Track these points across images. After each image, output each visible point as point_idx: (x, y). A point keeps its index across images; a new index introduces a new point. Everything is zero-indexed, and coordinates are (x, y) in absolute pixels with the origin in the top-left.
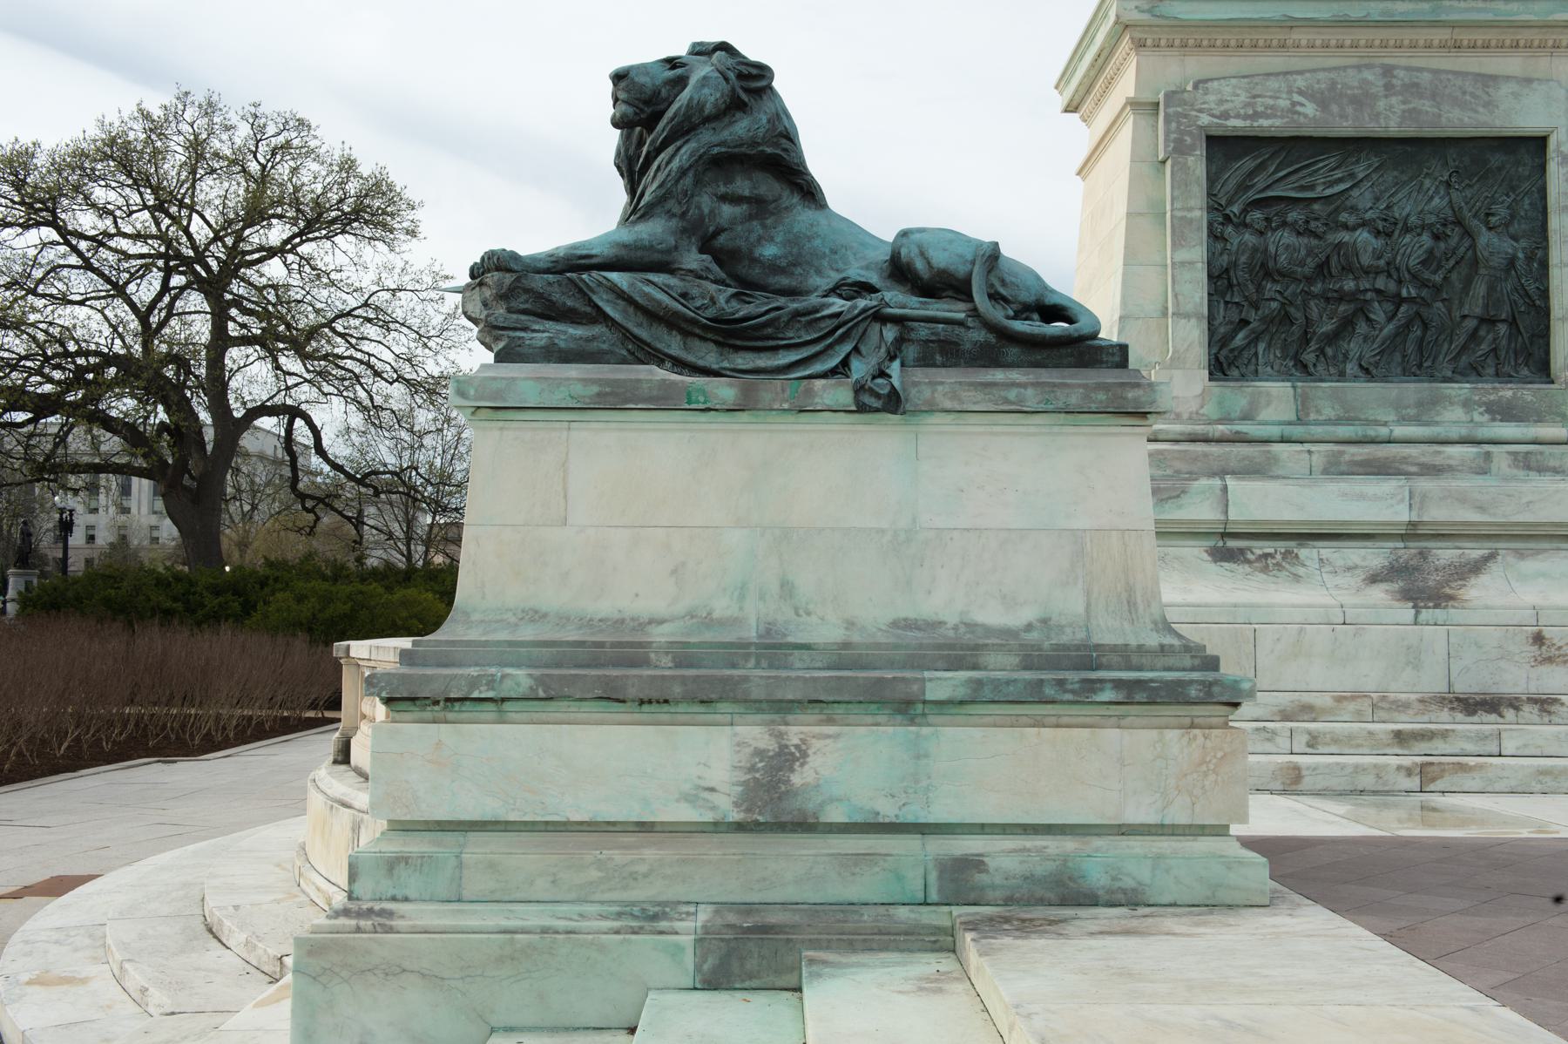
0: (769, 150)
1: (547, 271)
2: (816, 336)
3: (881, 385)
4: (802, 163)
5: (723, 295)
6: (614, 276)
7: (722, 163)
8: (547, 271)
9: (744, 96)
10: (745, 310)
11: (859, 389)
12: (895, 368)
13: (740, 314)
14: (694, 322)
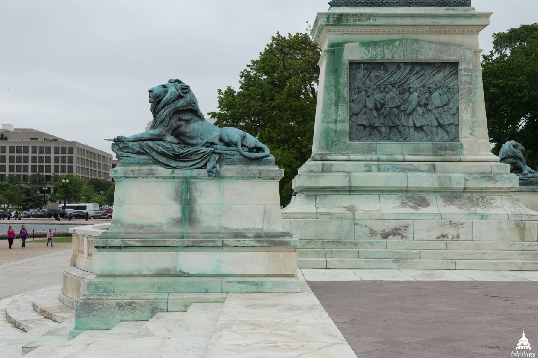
0: (189, 107)
1: (134, 141)
2: (199, 158)
3: (214, 171)
4: (199, 109)
5: (176, 147)
6: (149, 143)
7: (177, 112)
8: (134, 141)
9: (182, 95)
10: (182, 151)
11: (209, 171)
12: (218, 166)
13: (181, 152)
14: (169, 155)
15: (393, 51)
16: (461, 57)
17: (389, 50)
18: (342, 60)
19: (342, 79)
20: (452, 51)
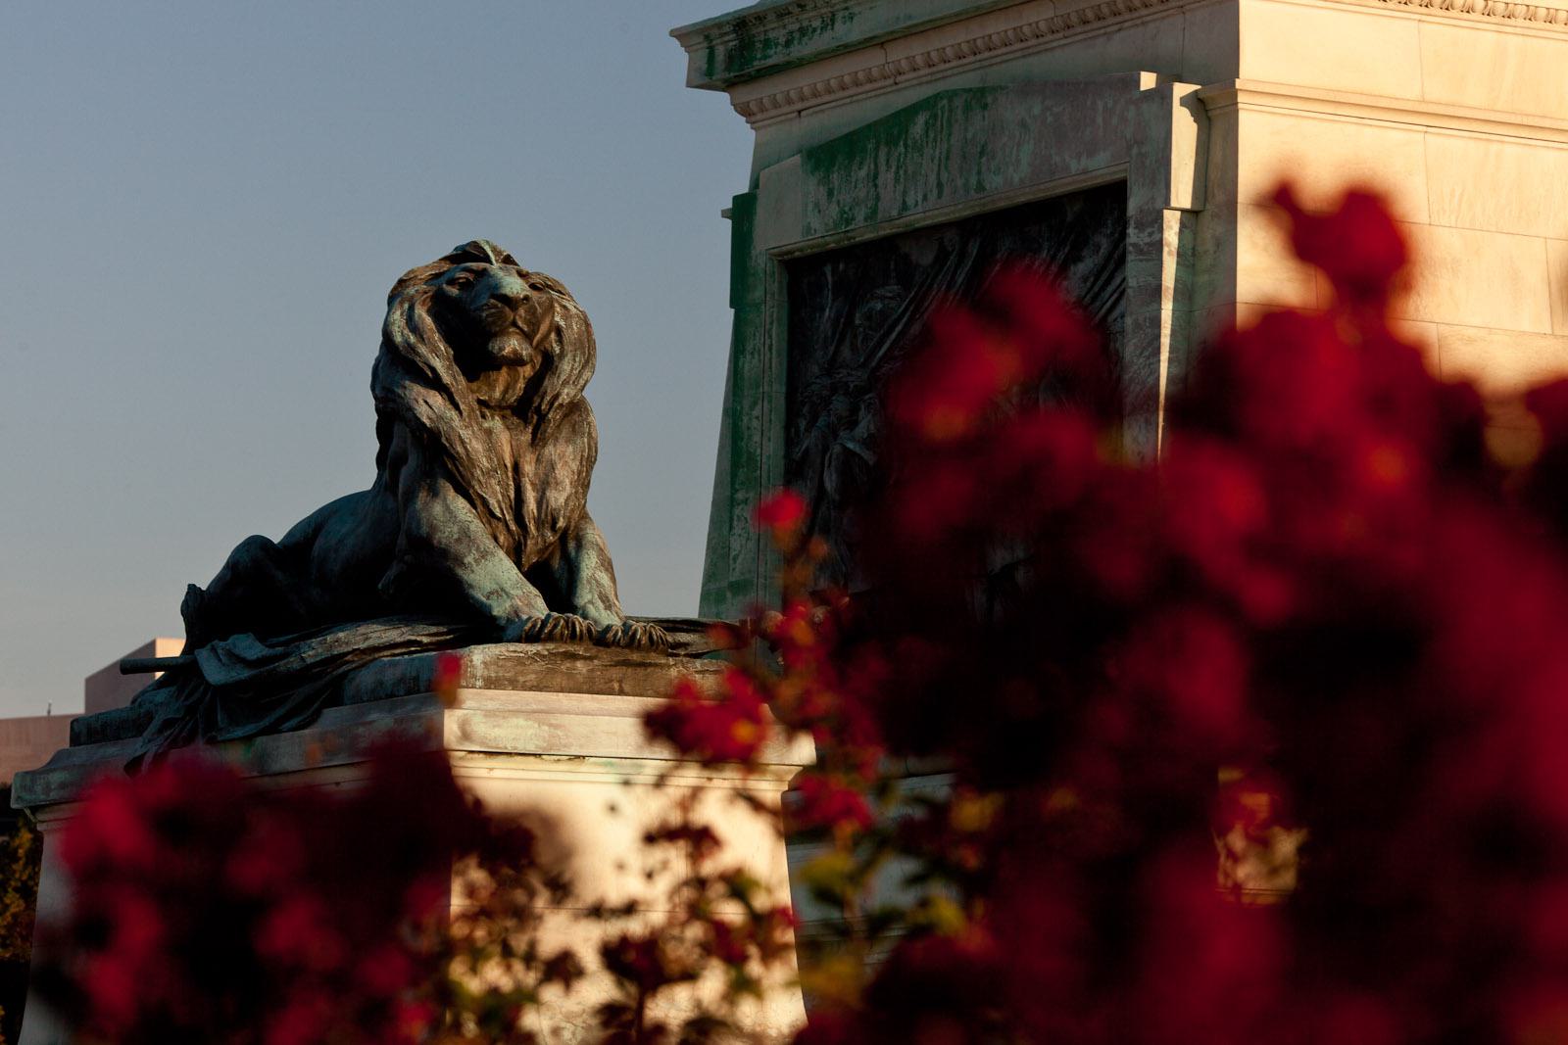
15: (906, 171)
16: (1129, 148)
17: (893, 169)
18: (751, 258)
19: (748, 357)
20: (1100, 120)
